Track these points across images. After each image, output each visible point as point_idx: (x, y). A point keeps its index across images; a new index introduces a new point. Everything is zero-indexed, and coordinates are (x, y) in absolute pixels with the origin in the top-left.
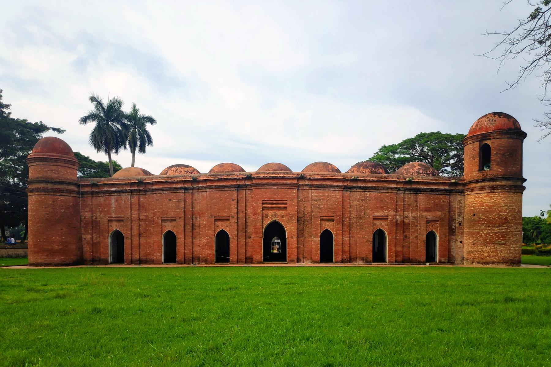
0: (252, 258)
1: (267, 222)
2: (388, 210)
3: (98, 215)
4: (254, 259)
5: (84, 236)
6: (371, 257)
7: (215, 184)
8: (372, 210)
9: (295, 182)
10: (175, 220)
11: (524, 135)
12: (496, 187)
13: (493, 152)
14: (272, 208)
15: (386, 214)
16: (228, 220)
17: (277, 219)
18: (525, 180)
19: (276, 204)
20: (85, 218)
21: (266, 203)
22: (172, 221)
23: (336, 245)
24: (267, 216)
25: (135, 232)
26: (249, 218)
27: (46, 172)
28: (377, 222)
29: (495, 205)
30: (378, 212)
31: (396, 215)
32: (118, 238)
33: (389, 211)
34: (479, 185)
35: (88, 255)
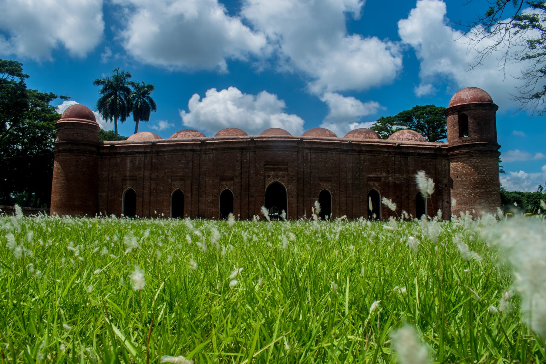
3: (114, 174)
14: (273, 170)
15: (379, 176)
16: (232, 180)
17: (278, 180)
18: (500, 146)
22: (181, 180)
25: (146, 192)
28: (371, 183)
30: (371, 174)
31: (388, 177)
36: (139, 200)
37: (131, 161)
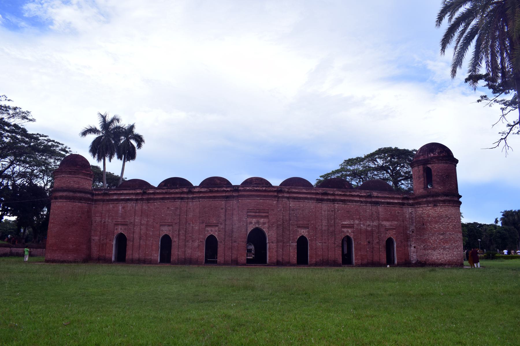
0: (237, 261)
1: (250, 228)
2: (353, 219)
3: (107, 219)
4: (239, 261)
5: (93, 238)
6: (340, 260)
7: (207, 195)
8: (341, 219)
9: (276, 194)
10: (172, 225)
11: (456, 161)
12: (440, 201)
13: (434, 173)
14: (255, 217)
15: (352, 223)
16: (217, 226)
17: (260, 226)
18: (461, 197)
19: (259, 212)
20: (95, 222)
21: (250, 212)
22: (169, 225)
23: (311, 249)
24: (251, 223)
25: (136, 236)
26: (235, 224)
27: (70, 182)
28: (345, 230)
29: (438, 217)
30: (345, 221)
31: (360, 224)
32: (122, 240)
33: (354, 220)
34: (425, 200)
35: (95, 252)
36: (129, 244)
37: (123, 208)
